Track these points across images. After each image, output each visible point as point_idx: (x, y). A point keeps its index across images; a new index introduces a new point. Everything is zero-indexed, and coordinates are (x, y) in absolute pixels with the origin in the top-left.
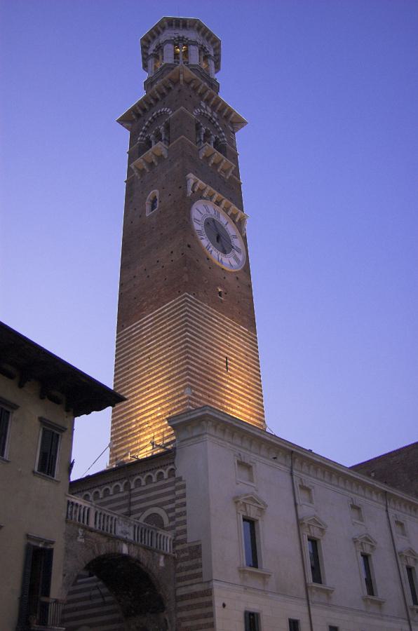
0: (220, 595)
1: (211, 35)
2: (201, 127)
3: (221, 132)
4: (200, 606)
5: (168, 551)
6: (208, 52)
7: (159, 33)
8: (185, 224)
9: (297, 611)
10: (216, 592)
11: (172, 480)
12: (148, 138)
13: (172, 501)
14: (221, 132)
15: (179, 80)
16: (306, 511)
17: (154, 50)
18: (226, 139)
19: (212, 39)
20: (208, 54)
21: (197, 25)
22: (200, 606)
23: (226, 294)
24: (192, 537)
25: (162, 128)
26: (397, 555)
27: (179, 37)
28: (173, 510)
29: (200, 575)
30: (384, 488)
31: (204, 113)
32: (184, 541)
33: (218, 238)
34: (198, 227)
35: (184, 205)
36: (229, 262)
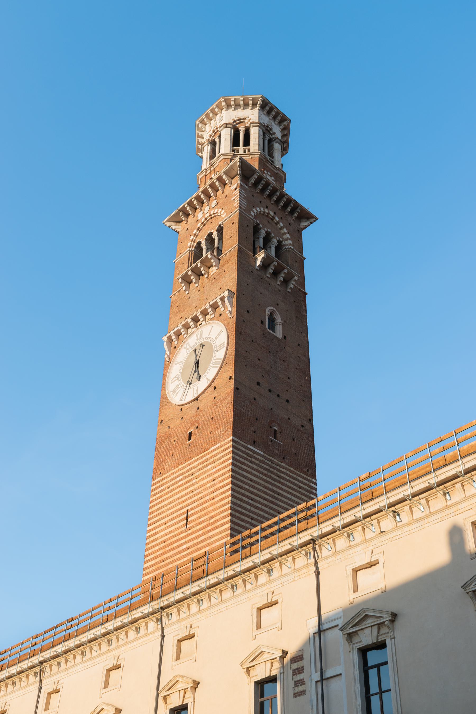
1: (278, 113)
2: (261, 229)
3: (285, 234)
6: (274, 133)
12: (199, 243)
17: (211, 136)
18: (290, 242)
19: (279, 118)
20: (274, 136)
23: (280, 432)
31: (264, 212)
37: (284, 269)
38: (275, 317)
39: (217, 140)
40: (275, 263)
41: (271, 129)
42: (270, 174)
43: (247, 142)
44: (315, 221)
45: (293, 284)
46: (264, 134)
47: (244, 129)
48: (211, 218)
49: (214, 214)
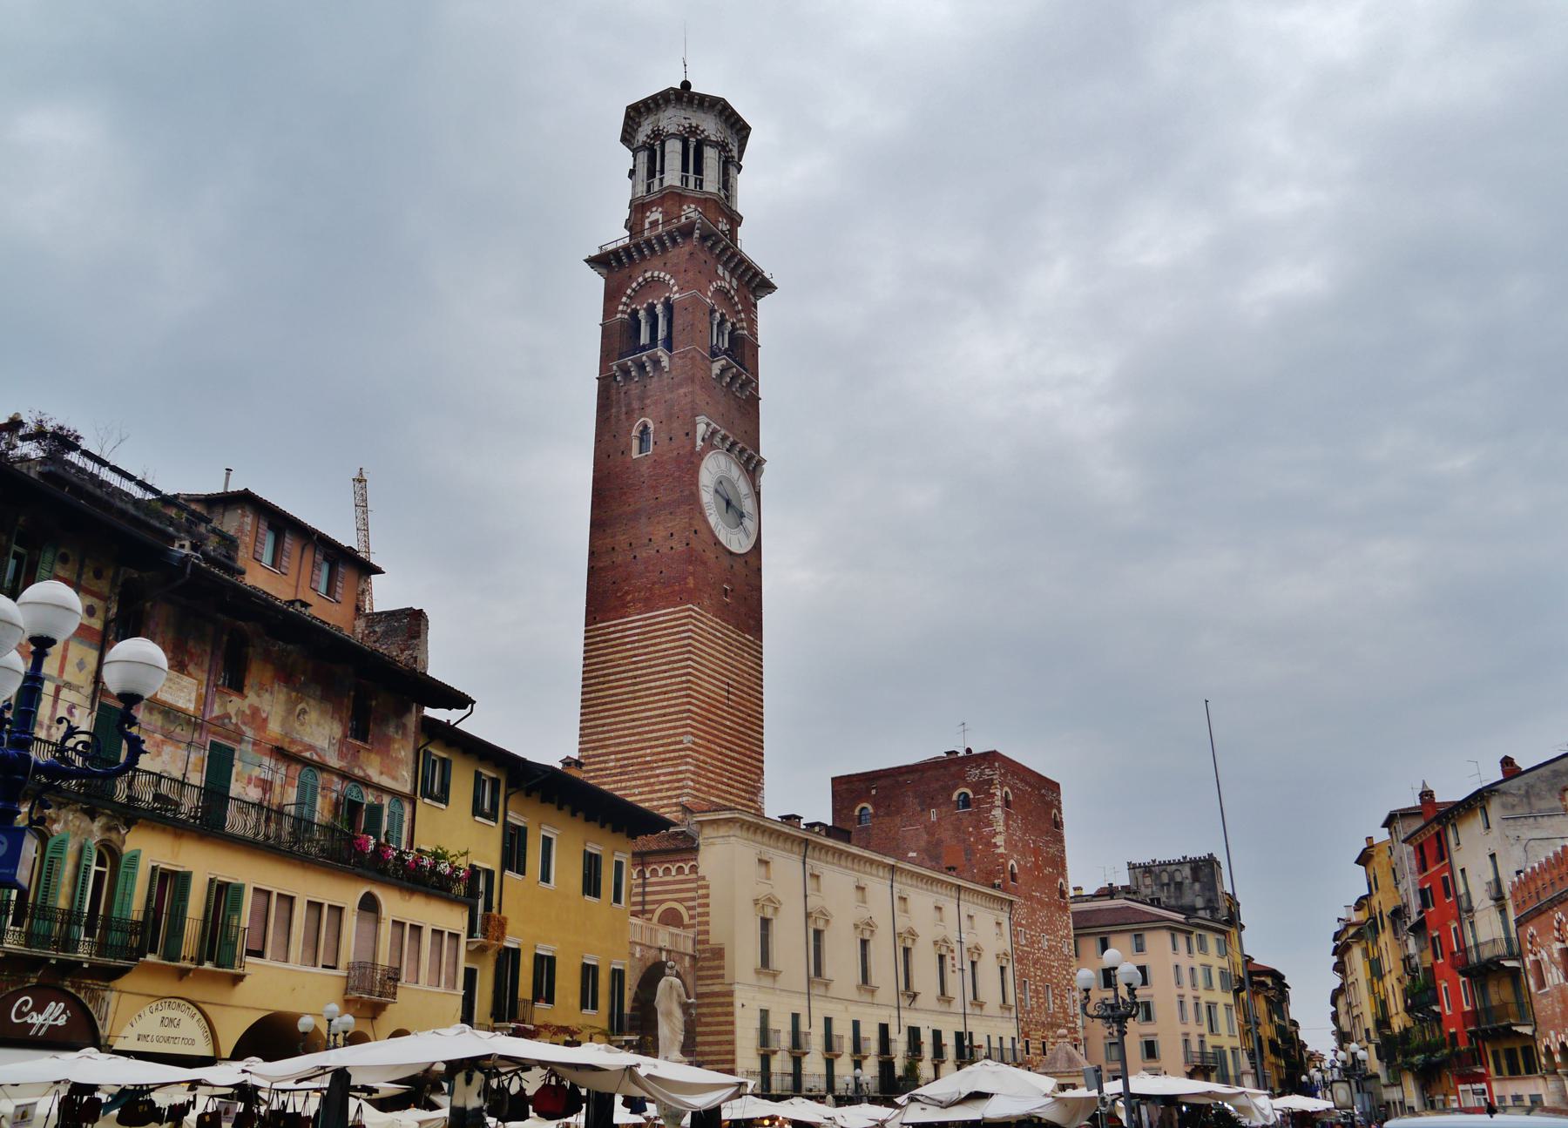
0: (740, 997)
3: (739, 312)
4: (722, 1005)
5: (690, 951)
8: (693, 499)
9: (799, 1005)
10: (738, 994)
11: (693, 876)
12: (635, 312)
13: (693, 899)
14: (739, 312)
16: (813, 902)
22: (722, 1005)
24: (715, 939)
25: (659, 308)
26: (896, 935)
28: (693, 908)
29: (722, 976)
30: (891, 861)
32: (706, 942)
33: (728, 503)
34: (707, 497)
35: (690, 464)
36: (738, 543)
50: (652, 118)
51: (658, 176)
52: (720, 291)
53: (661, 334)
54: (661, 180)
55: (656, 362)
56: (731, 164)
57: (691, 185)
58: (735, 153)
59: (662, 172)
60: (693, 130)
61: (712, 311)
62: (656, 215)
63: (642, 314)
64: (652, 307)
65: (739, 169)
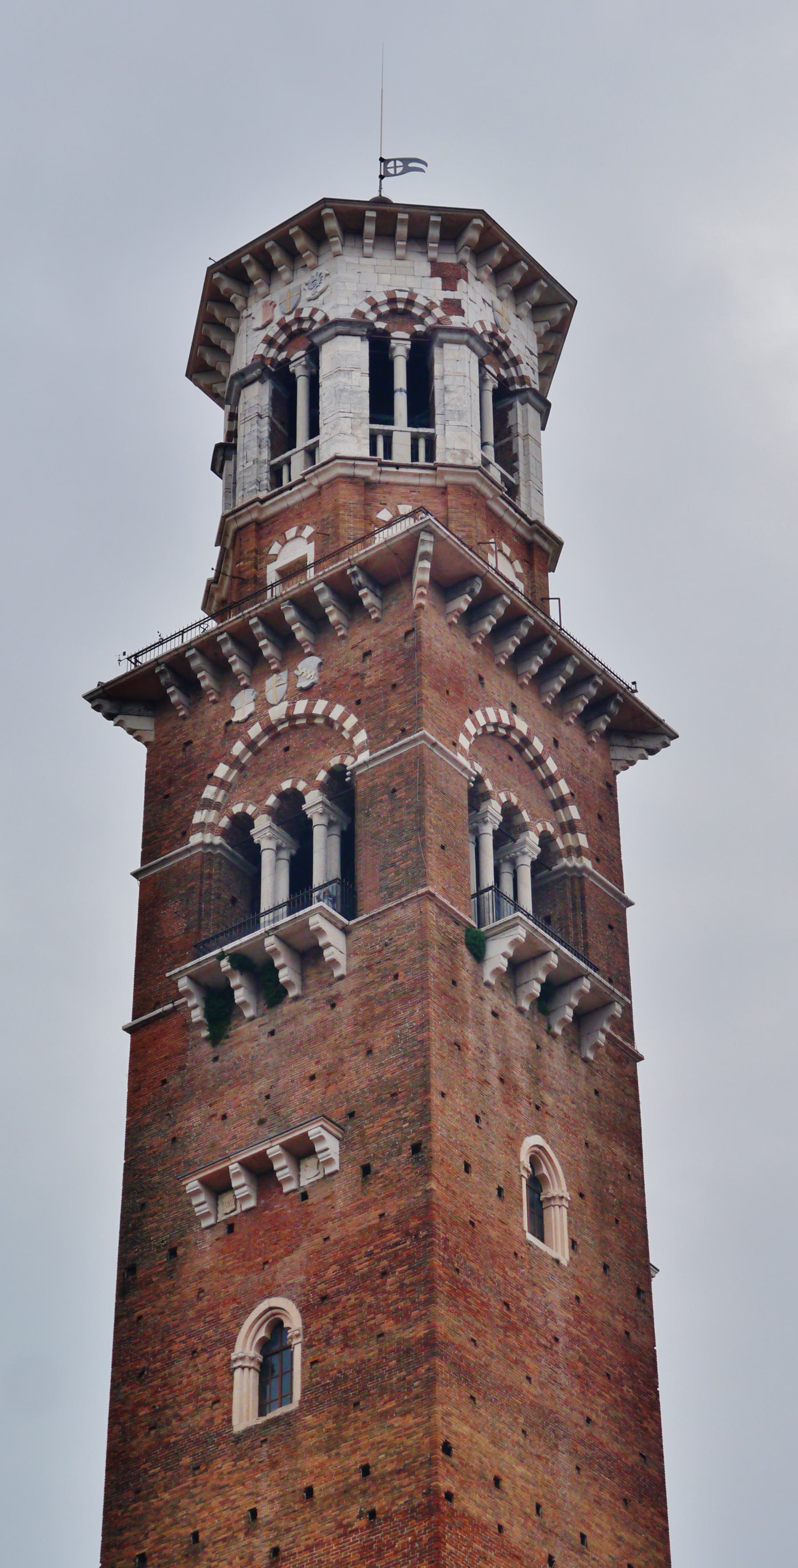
1: (536, 274)
6: (516, 361)
7: (293, 256)
12: (243, 823)
15: (408, 573)
17: (270, 342)
21: (472, 235)
25: (313, 799)
27: (392, 301)
37: (579, 976)
38: (545, 1171)
39: (298, 370)
40: (553, 960)
41: (505, 345)
42: (507, 550)
43: (422, 410)
44: (666, 745)
45: (603, 1031)
46: (482, 364)
47: (408, 345)
48: (294, 727)
49: (309, 716)
50: (279, 293)
51: (302, 440)
52: (497, 737)
53: (324, 863)
54: (311, 452)
55: (308, 954)
56: (513, 399)
57: (401, 451)
58: (529, 369)
59: (314, 429)
60: (400, 310)
61: (477, 796)
62: (297, 547)
63: (264, 831)
64: (293, 799)
65: (545, 409)
